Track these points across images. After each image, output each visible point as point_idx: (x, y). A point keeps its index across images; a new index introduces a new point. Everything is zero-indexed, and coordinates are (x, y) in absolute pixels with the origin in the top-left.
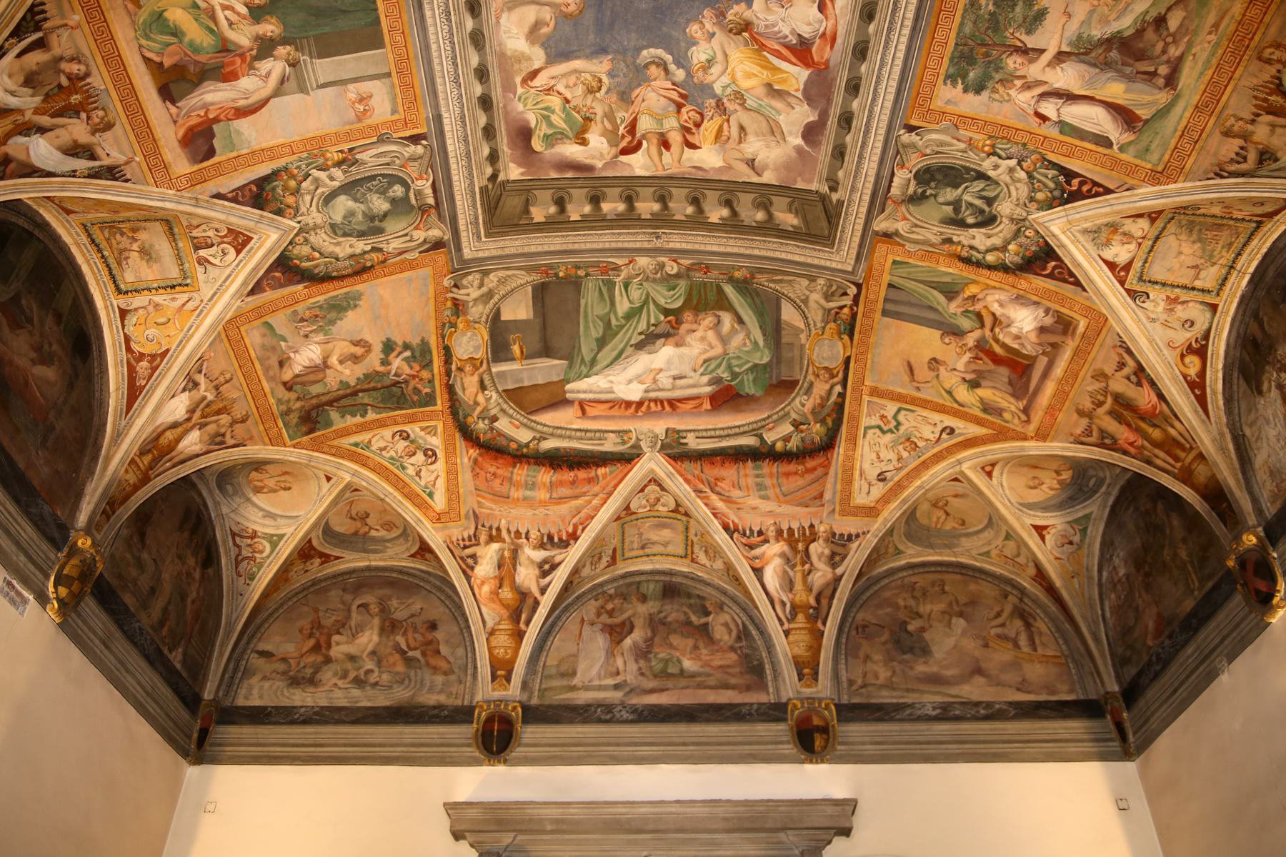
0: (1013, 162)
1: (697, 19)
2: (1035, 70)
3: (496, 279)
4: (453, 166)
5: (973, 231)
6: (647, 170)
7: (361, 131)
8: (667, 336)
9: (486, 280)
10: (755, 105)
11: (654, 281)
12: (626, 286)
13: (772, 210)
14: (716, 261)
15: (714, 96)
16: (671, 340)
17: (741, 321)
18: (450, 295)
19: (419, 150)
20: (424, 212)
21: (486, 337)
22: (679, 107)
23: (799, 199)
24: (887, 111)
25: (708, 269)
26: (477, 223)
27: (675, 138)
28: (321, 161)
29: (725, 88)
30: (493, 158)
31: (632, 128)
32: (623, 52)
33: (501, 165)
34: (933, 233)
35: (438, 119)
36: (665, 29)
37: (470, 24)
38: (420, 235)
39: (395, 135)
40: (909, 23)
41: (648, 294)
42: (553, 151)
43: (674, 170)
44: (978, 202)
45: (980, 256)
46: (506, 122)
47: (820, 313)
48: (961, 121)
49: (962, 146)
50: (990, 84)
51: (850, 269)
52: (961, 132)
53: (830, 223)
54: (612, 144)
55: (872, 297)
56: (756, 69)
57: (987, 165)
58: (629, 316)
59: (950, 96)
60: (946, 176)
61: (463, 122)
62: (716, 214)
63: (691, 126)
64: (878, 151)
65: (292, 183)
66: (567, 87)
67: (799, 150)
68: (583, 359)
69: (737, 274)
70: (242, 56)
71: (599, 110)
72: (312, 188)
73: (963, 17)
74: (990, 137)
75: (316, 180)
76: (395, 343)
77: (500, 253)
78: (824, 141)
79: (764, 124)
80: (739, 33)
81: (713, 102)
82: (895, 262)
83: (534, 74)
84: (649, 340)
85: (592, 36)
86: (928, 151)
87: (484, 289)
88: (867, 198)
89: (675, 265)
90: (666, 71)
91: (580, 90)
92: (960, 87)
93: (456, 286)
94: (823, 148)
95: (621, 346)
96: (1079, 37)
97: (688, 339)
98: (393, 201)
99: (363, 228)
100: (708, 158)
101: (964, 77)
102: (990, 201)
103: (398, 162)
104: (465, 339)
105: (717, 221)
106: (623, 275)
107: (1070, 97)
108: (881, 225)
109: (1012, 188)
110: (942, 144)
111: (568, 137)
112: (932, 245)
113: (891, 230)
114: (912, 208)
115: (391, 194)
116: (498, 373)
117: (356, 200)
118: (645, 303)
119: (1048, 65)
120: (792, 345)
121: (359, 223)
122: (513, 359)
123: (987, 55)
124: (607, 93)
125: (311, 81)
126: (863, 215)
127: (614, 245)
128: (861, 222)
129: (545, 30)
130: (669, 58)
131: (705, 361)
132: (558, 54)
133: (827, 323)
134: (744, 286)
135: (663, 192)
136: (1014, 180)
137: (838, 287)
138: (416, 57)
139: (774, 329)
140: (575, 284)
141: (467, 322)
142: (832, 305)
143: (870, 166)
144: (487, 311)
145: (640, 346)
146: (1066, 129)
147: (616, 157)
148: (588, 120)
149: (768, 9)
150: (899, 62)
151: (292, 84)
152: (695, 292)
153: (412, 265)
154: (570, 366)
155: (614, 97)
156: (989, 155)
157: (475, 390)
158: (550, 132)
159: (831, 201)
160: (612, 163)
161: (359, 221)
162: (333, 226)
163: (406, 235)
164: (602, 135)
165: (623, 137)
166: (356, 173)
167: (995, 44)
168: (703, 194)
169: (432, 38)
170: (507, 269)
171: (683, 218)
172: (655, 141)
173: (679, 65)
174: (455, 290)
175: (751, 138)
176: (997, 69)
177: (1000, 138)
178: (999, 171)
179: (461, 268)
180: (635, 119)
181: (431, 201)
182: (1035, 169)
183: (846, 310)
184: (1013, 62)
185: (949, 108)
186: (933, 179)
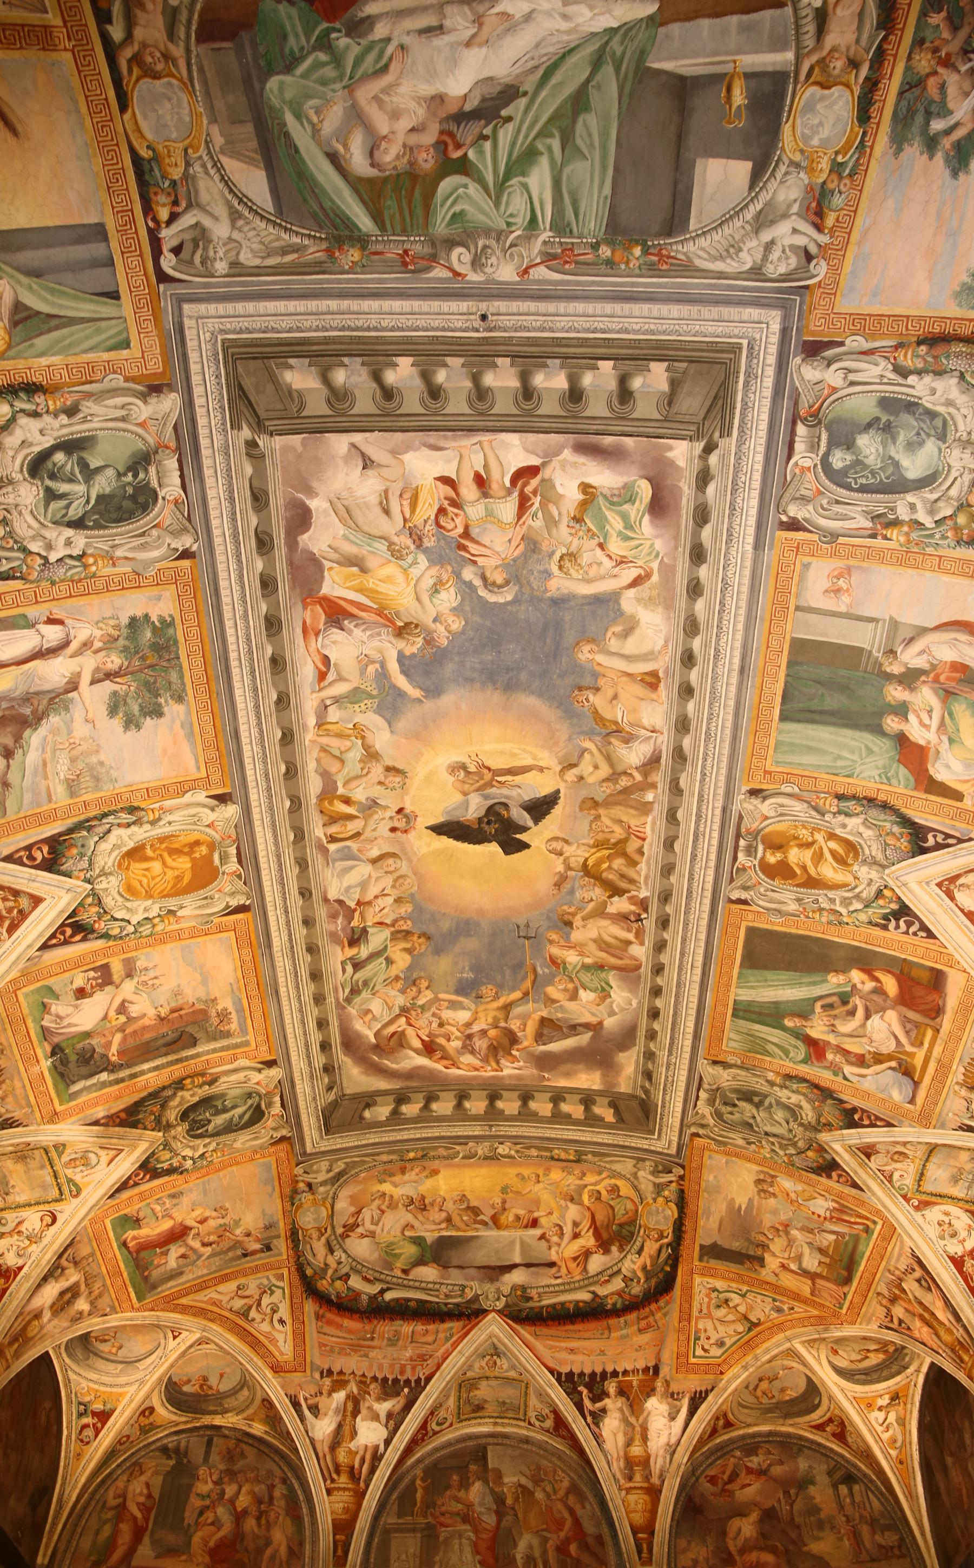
0: (53, 557)
1: (454, 635)
2: (88, 664)
3: (744, 255)
4: (757, 476)
5: (48, 442)
6: (503, 442)
7: (852, 556)
8: (461, 117)
9: (759, 257)
10: (376, 545)
11: (487, 232)
12: (533, 222)
13: (325, 392)
14: (393, 280)
15: (426, 551)
16: (453, 109)
17: (333, 158)
18: (823, 239)
19: (794, 511)
20: (815, 415)
21: (786, 129)
22: (466, 534)
23: (292, 417)
24: (221, 567)
25: (404, 262)
26: (748, 375)
27: (469, 491)
28: (914, 535)
29: (415, 563)
30: (704, 478)
31: (523, 504)
32: (535, 600)
33: (697, 465)
34: (97, 417)
35: (758, 545)
36: (488, 623)
37: (696, 644)
38: (833, 377)
39: (816, 537)
40: (234, 663)
41: (497, 205)
42: (625, 479)
43: (467, 442)
44: (64, 488)
45: (19, 405)
46: (678, 526)
47: (204, 197)
48: (136, 581)
49: (119, 553)
50: (125, 632)
51: (186, 307)
52: (129, 569)
53: (241, 387)
54: (548, 482)
55: (134, 261)
56: (383, 588)
57: (80, 540)
58: (528, 157)
59: (160, 605)
60: (120, 508)
61: (730, 534)
62: (402, 373)
63: (450, 509)
64: (213, 514)
65: (961, 520)
66: (600, 564)
67: (311, 492)
68: (617, 69)
69: (354, 254)
70: (936, 680)
71: (563, 531)
72: (941, 504)
73: (183, 684)
74: (94, 575)
75: (931, 512)
76: (947, 160)
77: (727, 311)
78: (282, 510)
79: (360, 520)
80: (407, 624)
81: (427, 543)
82: (126, 344)
83: (636, 582)
84: (493, 105)
85: (568, 618)
86: (155, 532)
87: (766, 236)
88: (204, 442)
89: (457, 267)
90: (484, 578)
91: (585, 558)
92: (154, 618)
93: (809, 257)
94: (281, 502)
95: (543, 94)
96: (67, 709)
97: (421, 112)
98: (850, 446)
99: (906, 418)
100: (425, 464)
101: (155, 630)
102: (51, 496)
103: (825, 502)
104: (825, 132)
105: (400, 360)
106: (538, 245)
107: (40, 654)
108: (169, 403)
109: (35, 525)
110: (143, 547)
111: (605, 496)
112: (89, 395)
113: (153, 400)
114: (141, 445)
115: (849, 458)
116: (783, 48)
117: (896, 464)
118: (501, 186)
119: (79, 674)
120: (235, 121)
121: (907, 427)
122: (748, 76)
123: (143, 658)
124: (553, 553)
125: (882, 631)
126: (200, 412)
127: (551, 307)
128: (199, 401)
129: (618, 629)
130: (482, 592)
131: (385, 69)
132: (605, 604)
133: (186, 176)
134: (341, 234)
135: (481, 406)
136: (38, 536)
137: (191, 262)
138: (762, 620)
139: (273, 150)
140: (616, 231)
141: (811, 170)
142: (187, 220)
143: (215, 490)
144: (773, 185)
145: (510, 93)
146: (22, 623)
147: (544, 464)
148: (578, 520)
149: (380, 652)
150: (229, 624)
151: (903, 634)
152: (419, 211)
153: (866, 324)
154: (642, 54)
155: (545, 546)
156: (84, 555)
157: (839, 11)
158: (626, 507)
159: (250, 425)
160: (550, 454)
161: (908, 425)
162: (942, 437)
163: (852, 384)
164: (561, 496)
165: (535, 493)
166: (879, 503)
167: (141, 671)
168: (425, 406)
169: (739, 636)
170: (721, 275)
171: (449, 360)
172: (495, 486)
173: (469, 585)
174: (813, 249)
175: (373, 499)
176: (125, 649)
177: (83, 579)
178: (62, 540)
179: (792, 295)
180: (520, 515)
181: (801, 430)
182: (24, 561)
183: (164, 214)
184: (115, 661)
185: (154, 591)
186: (133, 498)
